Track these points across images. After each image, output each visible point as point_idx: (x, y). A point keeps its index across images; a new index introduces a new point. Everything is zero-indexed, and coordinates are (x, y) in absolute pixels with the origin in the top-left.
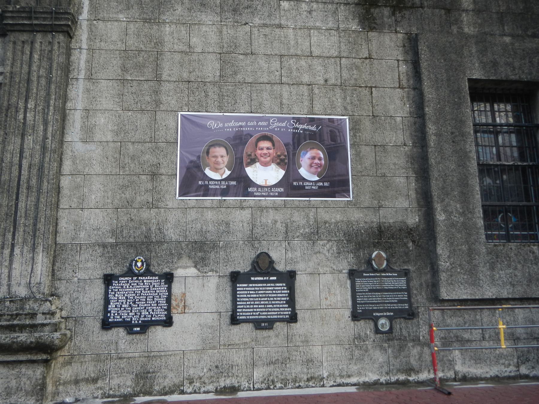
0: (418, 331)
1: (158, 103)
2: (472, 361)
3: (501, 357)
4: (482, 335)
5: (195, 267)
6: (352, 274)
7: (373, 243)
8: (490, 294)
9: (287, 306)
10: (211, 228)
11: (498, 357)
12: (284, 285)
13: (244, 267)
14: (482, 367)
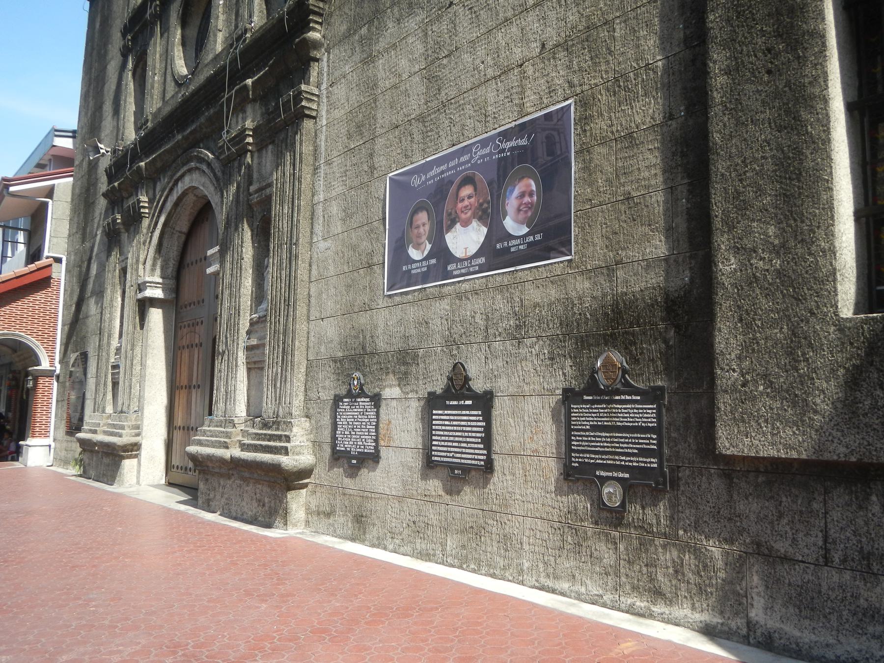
0: (676, 517)
2: (791, 610)
3: (873, 617)
4: (822, 552)
5: (399, 385)
7: (605, 335)
8: (842, 450)
9: (482, 446)
10: (413, 332)
11: (864, 614)
12: (480, 413)
14: (814, 628)
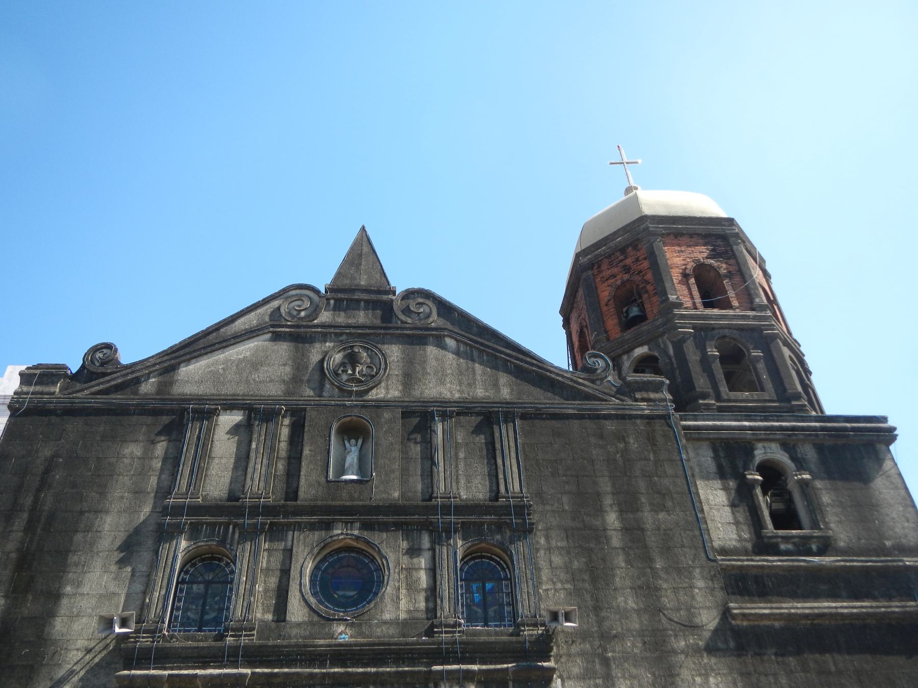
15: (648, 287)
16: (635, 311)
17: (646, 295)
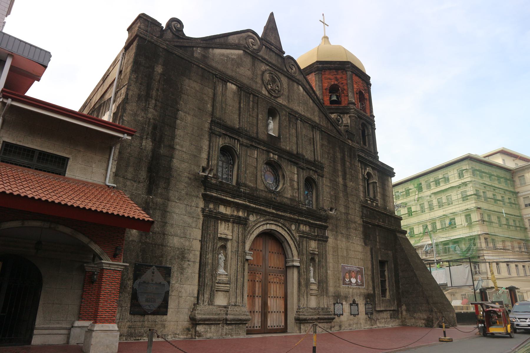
1: (338, 261)
6: (365, 305)
13: (352, 302)
15: (344, 91)
16: (334, 98)
17: (343, 94)
